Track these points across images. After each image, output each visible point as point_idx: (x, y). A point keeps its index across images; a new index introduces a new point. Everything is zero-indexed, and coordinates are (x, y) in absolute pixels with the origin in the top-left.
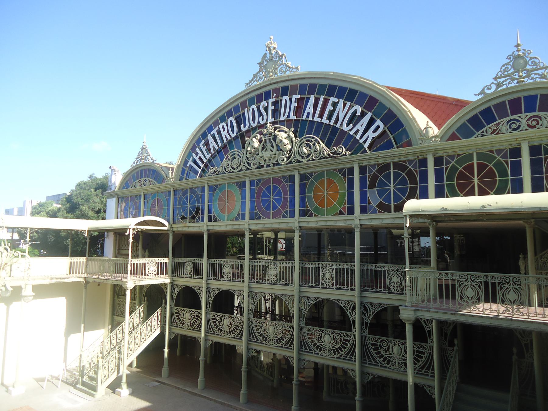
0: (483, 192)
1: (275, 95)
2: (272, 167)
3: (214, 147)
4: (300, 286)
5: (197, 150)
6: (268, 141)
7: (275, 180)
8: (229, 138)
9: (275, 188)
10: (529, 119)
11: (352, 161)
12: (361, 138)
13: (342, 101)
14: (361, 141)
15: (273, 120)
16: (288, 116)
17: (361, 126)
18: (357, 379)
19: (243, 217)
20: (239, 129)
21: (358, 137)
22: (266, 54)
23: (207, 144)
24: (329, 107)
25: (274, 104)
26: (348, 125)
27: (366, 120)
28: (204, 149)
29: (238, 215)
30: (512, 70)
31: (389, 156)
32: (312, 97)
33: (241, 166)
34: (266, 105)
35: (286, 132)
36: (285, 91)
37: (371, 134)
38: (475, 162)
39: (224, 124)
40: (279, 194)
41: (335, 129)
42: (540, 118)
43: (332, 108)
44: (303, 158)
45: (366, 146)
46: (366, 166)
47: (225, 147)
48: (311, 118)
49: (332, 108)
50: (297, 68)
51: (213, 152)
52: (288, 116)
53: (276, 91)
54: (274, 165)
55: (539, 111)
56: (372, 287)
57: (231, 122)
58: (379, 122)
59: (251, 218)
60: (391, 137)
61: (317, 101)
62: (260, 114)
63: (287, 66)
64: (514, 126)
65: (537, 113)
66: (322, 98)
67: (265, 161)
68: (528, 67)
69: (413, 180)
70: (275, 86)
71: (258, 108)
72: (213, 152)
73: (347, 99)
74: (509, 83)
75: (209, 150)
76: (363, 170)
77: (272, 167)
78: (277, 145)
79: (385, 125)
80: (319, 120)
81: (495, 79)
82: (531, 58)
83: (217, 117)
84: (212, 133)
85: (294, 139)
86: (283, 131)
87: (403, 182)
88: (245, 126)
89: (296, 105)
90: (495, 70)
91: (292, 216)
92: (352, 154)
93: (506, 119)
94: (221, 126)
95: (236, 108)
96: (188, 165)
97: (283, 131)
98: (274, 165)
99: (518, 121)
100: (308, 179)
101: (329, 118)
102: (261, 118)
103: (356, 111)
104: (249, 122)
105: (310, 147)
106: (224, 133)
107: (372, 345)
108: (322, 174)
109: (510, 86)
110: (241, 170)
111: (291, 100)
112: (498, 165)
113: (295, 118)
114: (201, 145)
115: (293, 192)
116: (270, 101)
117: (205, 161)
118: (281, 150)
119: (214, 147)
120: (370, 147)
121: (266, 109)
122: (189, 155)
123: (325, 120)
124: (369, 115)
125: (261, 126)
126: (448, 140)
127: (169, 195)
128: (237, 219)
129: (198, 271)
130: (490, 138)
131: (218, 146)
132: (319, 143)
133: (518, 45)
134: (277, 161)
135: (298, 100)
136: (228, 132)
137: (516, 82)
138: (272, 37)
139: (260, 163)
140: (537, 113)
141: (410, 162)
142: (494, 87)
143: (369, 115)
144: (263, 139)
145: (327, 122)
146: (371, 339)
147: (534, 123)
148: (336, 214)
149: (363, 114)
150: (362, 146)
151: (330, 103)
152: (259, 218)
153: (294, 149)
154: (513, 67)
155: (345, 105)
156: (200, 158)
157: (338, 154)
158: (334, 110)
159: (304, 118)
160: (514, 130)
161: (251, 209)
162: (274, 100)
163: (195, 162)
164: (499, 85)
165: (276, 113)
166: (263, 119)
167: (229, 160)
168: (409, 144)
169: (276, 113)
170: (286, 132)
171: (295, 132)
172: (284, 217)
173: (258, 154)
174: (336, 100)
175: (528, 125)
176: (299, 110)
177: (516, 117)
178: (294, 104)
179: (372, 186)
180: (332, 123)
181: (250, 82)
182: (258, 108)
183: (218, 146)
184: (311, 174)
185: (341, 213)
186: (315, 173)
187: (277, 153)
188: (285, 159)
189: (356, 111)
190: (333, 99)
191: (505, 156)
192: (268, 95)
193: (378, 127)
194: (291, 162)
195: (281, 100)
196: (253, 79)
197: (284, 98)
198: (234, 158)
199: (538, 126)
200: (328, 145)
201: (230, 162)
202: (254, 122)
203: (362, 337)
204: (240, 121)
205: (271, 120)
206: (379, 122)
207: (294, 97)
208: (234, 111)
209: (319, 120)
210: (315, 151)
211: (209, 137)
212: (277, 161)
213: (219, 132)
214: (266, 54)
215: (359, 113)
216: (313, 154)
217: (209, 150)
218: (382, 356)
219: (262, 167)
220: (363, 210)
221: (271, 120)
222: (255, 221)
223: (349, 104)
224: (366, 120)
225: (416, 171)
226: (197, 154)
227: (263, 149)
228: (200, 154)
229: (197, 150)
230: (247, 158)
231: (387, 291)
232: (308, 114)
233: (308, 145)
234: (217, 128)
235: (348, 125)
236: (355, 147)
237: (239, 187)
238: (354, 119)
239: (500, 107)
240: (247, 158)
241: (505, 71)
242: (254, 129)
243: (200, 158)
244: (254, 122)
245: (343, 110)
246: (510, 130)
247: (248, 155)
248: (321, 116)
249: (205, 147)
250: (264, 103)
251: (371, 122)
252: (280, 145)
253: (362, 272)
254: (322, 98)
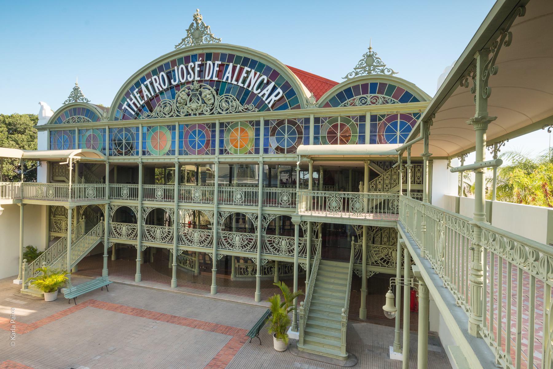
0: (342, 142)
1: (201, 59)
2: (198, 116)
3: (147, 95)
4: (219, 204)
5: (131, 96)
6: (195, 95)
7: (200, 126)
8: (161, 89)
9: (200, 132)
10: (371, 98)
11: (259, 116)
12: (266, 100)
13: (253, 71)
14: (267, 102)
15: (199, 79)
16: (212, 77)
17: (266, 91)
18: (258, 264)
19: (173, 152)
21: (264, 99)
22: (193, 23)
23: (140, 92)
24: (244, 74)
25: (200, 66)
26: (257, 90)
27: (270, 87)
28: (138, 96)
29: (169, 151)
30: (365, 65)
31: (285, 115)
32: (231, 65)
33: (172, 113)
34: (193, 66)
35: (209, 89)
36: (209, 57)
37: (273, 98)
38: (339, 122)
39: (156, 77)
40: (203, 136)
41: (247, 92)
42: (378, 98)
43: (246, 75)
44: (222, 110)
45: (270, 106)
46: (269, 120)
47: (157, 96)
48: (229, 81)
49: (246, 75)
50: (219, 40)
51: (146, 99)
52: (212, 77)
53: (201, 55)
54: (200, 114)
55: (378, 93)
56: (270, 203)
57: (162, 76)
58: (279, 90)
59: (180, 154)
60: (287, 101)
61: (234, 68)
62: (188, 73)
63: (211, 36)
64: (363, 101)
65: (376, 95)
66: (238, 66)
67: (192, 110)
68: (374, 64)
69: (300, 133)
70: (200, 52)
71: (187, 68)
72: (146, 99)
73: (257, 70)
74: (363, 73)
75: (142, 97)
76: (267, 123)
77: (198, 116)
78: (202, 99)
79: (283, 92)
80: (236, 83)
81: (355, 69)
82: (377, 58)
83: (150, 70)
84: (145, 83)
85: (215, 95)
86: (207, 88)
87: (293, 133)
88: (175, 81)
89: (218, 69)
90: (356, 63)
91: (213, 153)
92: (259, 111)
93: (359, 97)
94: (153, 78)
95: (167, 65)
96: (123, 108)
97: (207, 88)
98: (200, 114)
99: (366, 98)
100: (226, 127)
101: (244, 82)
102: (189, 76)
103: (264, 79)
104: (178, 79)
105: (228, 103)
106: (156, 85)
107: (268, 241)
108: (237, 123)
109: (363, 75)
110: (172, 116)
111: (214, 64)
112: (353, 125)
113: (216, 79)
114: (135, 92)
115: (214, 136)
116: (197, 63)
117: (139, 106)
118: (205, 103)
119: (147, 95)
120: (272, 107)
121: (193, 69)
122: (124, 100)
123: (240, 84)
124: (273, 84)
125: (188, 83)
126: (324, 107)
127: (105, 132)
128: (168, 154)
129: (133, 194)
130: (349, 108)
131: (151, 95)
132: (235, 100)
133: (370, 48)
134: (202, 111)
135: (219, 66)
136: (160, 84)
137: (367, 72)
138: (198, 10)
139: (188, 112)
140: (376, 95)
141: (299, 119)
142: (354, 74)
143: (273, 84)
144: (191, 93)
145: (242, 85)
146: (267, 237)
147: (374, 101)
148: (246, 153)
149: (268, 83)
150: (266, 106)
151: (245, 71)
152: (187, 154)
153: (216, 103)
154: (366, 62)
155: (255, 74)
156: (134, 103)
157: (249, 110)
158: (247, 77)
159: (224, 80)
160: (363, 104)
161: (180, 146)
162: (200, 63)
163: (129, 105)
164: (357, 74)
165: (201, 73)
166: (190, 77)
167: (161, 107)
168: (299, 107)
169: (201, 73)
170: (209, 89)
171: (217, 91)
172: (207, 154)
173: (186, 105)
174: (249, 69)
175: (371, 102)
176: (220, 73)
177: (365, 96)
178: (217, 69)
179: (273, 135)
180: (245, 87)
181: (179, 44)
182: (187, 68)
183: (151, 95)
184: (228, 123)
185: (250, 153)
186: (232, 122)
187: (202, 105)
188: (209, 111)
189: (264, 79)
190: (246, 69)
191: (356, 121)
192: (194, 58)
193: (279, 93)
194: (213, 114)
195: (206, 64)
196: (181, 43)
197: (209, 62)
198: (166, 106)
199: (377, 103)
200: (242, 103)
201: (162, 109)
202: (183, 79)
203: (262, 237)
205: (197, 78)
206: (279, 90)
207: (217, 63)
208: (165, 66)
209: (236, 83)
210: (232, 106)
211: (143, 86)
212: (202, 111)
213: (151, 83)
214: (193, 23)
215: (265, 81)
216: (230, 108)
217: (142, 97)
218: (275, 247)
219: (190, 115)
220: (266, 151)
221: (197, 78)
222: (184, 156)
223: (258, 73)
224: (270, 87)
225: (302, 126)
226: (131, 100)
227: (190, 101)
228: (134, 100)
229: (131, 96)
230: (177, 107)
231: (279, 205)
232: (228, 77)
233: (226, 101)
234: (150, 80)
235: (257, 90)
236: (261, 106)
237: (170, 130)
238: (262, 86)
239: (356, 88)
240: (177, 107)
241: (361, 64)
242: (183, 84)
243: (134, 103)
244: (183, 79)
245: (254, 78)
246: (361, 104)
247: (178, 105)
248: (237, 80)
249: (139, 95)
251: (274, 89)
252: (205, 99)
253: (263, 193)
254: (238, 66)
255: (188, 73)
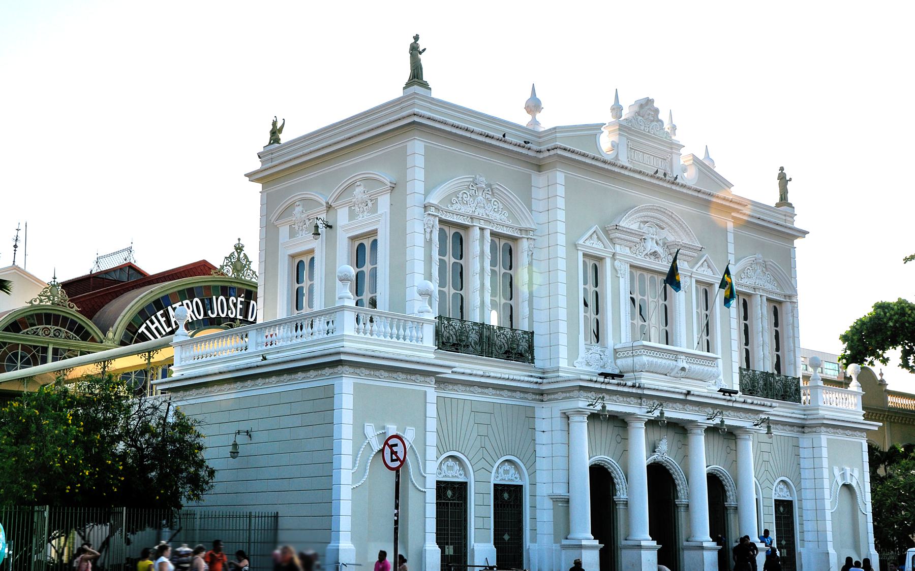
20: (206, 314)
23: (166, 315)
28: (162, 320)
62: (229, 308)
84: (174, 306)
96: (140, 331)
116: (239, 299)
121: (235, 305)
136: (193, 311)
156: (156, 328)
204: (208, 305)
226: (153, 323)
228: (157, 324)
243: (156, 328)
250: (232, 298)
255: (229, 308)
